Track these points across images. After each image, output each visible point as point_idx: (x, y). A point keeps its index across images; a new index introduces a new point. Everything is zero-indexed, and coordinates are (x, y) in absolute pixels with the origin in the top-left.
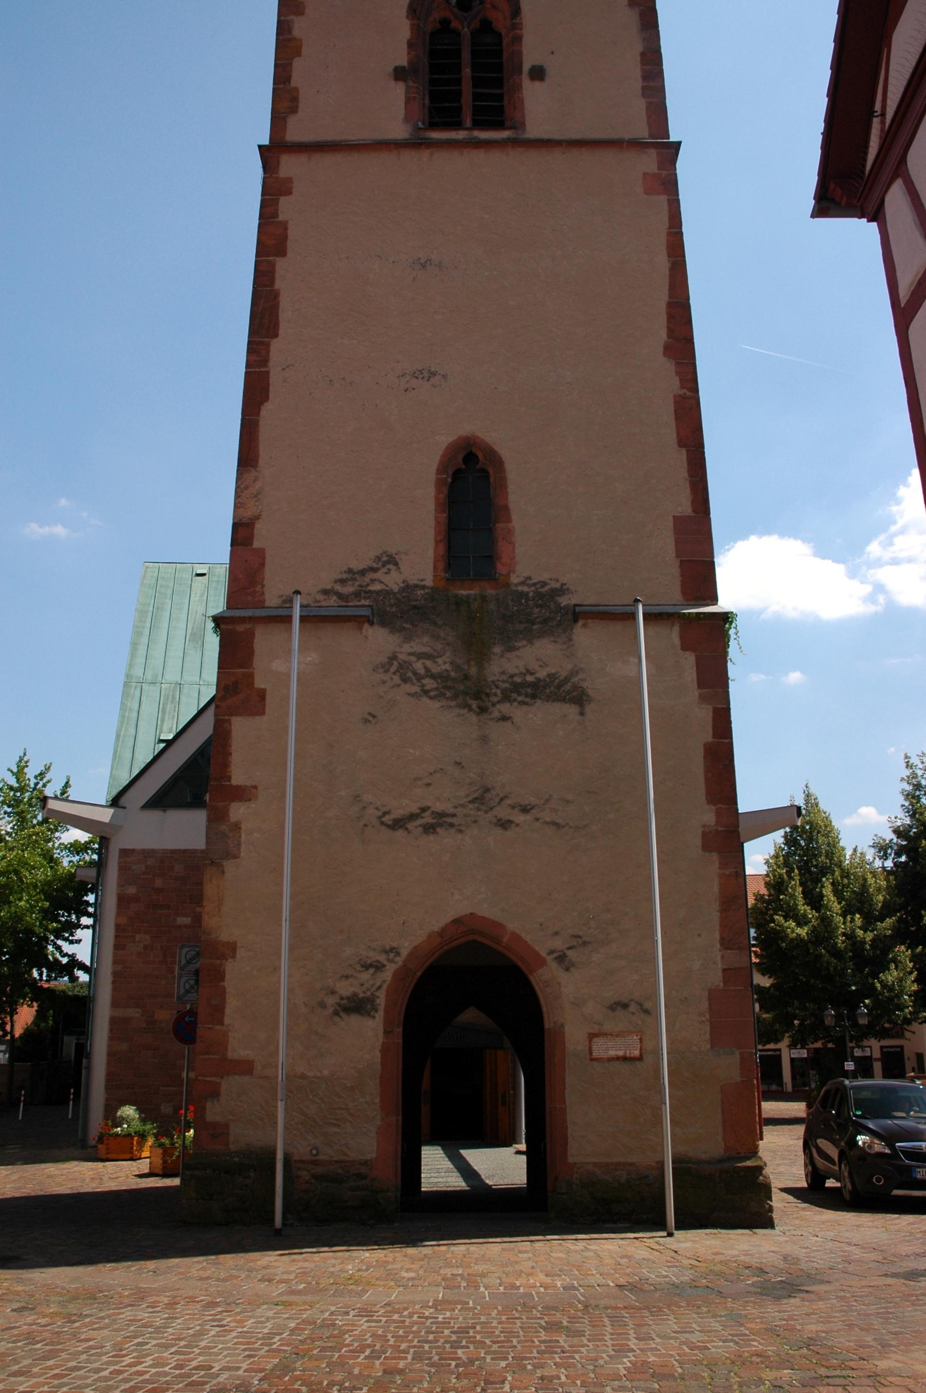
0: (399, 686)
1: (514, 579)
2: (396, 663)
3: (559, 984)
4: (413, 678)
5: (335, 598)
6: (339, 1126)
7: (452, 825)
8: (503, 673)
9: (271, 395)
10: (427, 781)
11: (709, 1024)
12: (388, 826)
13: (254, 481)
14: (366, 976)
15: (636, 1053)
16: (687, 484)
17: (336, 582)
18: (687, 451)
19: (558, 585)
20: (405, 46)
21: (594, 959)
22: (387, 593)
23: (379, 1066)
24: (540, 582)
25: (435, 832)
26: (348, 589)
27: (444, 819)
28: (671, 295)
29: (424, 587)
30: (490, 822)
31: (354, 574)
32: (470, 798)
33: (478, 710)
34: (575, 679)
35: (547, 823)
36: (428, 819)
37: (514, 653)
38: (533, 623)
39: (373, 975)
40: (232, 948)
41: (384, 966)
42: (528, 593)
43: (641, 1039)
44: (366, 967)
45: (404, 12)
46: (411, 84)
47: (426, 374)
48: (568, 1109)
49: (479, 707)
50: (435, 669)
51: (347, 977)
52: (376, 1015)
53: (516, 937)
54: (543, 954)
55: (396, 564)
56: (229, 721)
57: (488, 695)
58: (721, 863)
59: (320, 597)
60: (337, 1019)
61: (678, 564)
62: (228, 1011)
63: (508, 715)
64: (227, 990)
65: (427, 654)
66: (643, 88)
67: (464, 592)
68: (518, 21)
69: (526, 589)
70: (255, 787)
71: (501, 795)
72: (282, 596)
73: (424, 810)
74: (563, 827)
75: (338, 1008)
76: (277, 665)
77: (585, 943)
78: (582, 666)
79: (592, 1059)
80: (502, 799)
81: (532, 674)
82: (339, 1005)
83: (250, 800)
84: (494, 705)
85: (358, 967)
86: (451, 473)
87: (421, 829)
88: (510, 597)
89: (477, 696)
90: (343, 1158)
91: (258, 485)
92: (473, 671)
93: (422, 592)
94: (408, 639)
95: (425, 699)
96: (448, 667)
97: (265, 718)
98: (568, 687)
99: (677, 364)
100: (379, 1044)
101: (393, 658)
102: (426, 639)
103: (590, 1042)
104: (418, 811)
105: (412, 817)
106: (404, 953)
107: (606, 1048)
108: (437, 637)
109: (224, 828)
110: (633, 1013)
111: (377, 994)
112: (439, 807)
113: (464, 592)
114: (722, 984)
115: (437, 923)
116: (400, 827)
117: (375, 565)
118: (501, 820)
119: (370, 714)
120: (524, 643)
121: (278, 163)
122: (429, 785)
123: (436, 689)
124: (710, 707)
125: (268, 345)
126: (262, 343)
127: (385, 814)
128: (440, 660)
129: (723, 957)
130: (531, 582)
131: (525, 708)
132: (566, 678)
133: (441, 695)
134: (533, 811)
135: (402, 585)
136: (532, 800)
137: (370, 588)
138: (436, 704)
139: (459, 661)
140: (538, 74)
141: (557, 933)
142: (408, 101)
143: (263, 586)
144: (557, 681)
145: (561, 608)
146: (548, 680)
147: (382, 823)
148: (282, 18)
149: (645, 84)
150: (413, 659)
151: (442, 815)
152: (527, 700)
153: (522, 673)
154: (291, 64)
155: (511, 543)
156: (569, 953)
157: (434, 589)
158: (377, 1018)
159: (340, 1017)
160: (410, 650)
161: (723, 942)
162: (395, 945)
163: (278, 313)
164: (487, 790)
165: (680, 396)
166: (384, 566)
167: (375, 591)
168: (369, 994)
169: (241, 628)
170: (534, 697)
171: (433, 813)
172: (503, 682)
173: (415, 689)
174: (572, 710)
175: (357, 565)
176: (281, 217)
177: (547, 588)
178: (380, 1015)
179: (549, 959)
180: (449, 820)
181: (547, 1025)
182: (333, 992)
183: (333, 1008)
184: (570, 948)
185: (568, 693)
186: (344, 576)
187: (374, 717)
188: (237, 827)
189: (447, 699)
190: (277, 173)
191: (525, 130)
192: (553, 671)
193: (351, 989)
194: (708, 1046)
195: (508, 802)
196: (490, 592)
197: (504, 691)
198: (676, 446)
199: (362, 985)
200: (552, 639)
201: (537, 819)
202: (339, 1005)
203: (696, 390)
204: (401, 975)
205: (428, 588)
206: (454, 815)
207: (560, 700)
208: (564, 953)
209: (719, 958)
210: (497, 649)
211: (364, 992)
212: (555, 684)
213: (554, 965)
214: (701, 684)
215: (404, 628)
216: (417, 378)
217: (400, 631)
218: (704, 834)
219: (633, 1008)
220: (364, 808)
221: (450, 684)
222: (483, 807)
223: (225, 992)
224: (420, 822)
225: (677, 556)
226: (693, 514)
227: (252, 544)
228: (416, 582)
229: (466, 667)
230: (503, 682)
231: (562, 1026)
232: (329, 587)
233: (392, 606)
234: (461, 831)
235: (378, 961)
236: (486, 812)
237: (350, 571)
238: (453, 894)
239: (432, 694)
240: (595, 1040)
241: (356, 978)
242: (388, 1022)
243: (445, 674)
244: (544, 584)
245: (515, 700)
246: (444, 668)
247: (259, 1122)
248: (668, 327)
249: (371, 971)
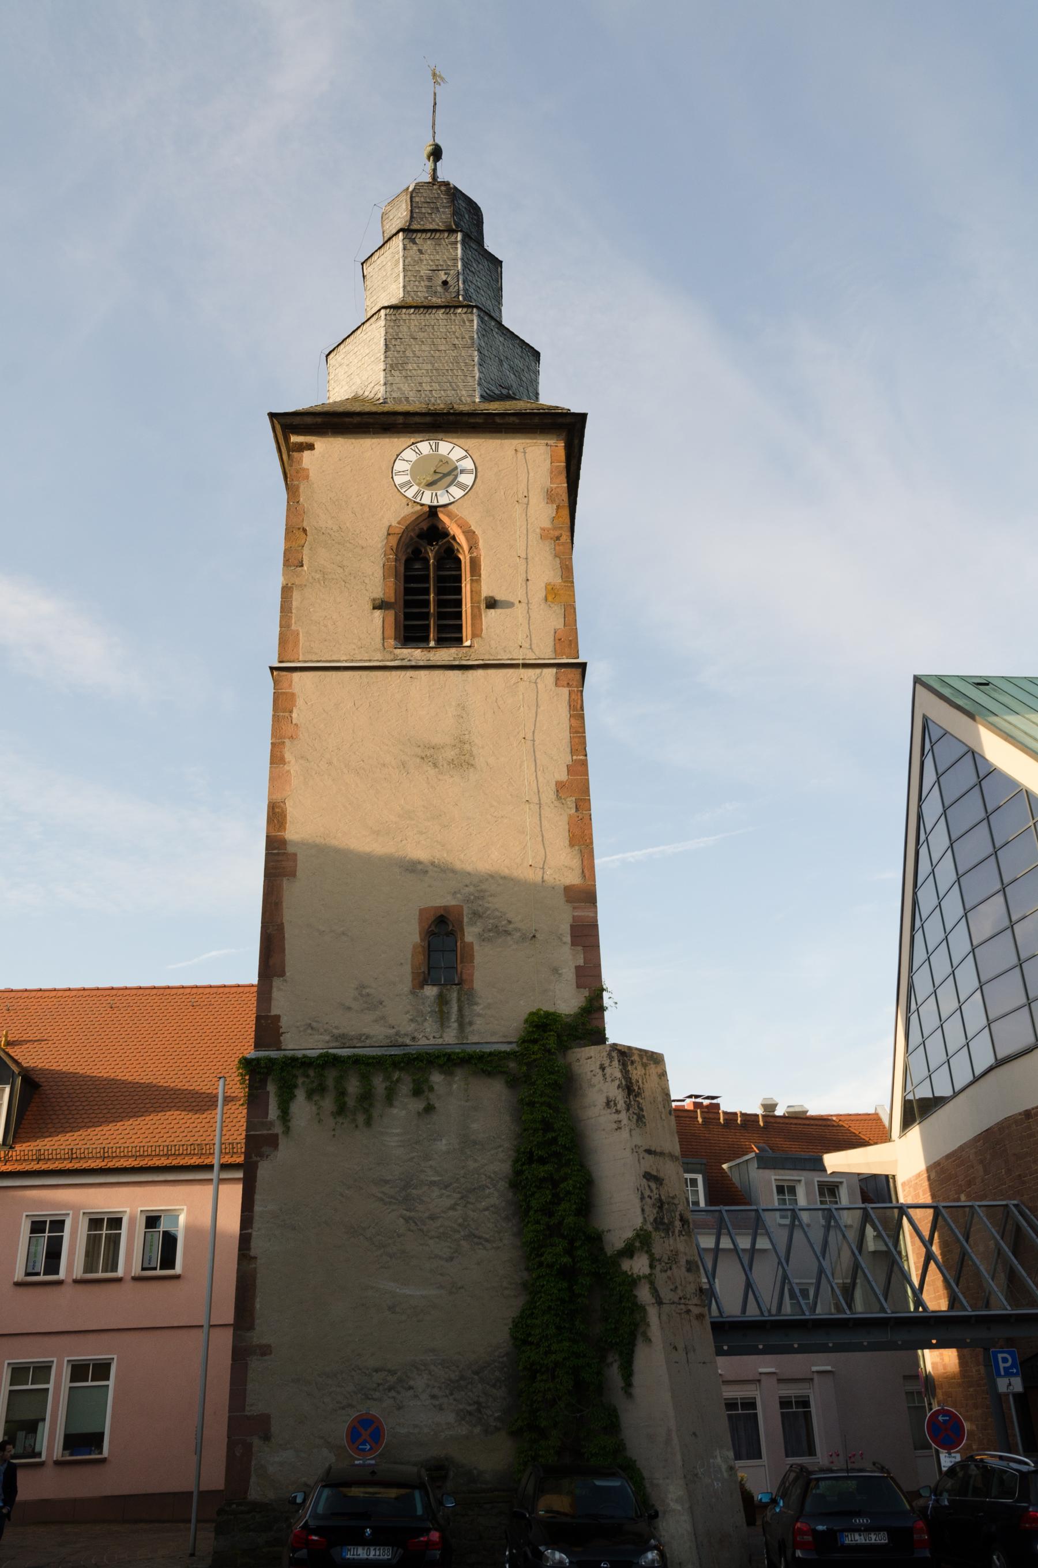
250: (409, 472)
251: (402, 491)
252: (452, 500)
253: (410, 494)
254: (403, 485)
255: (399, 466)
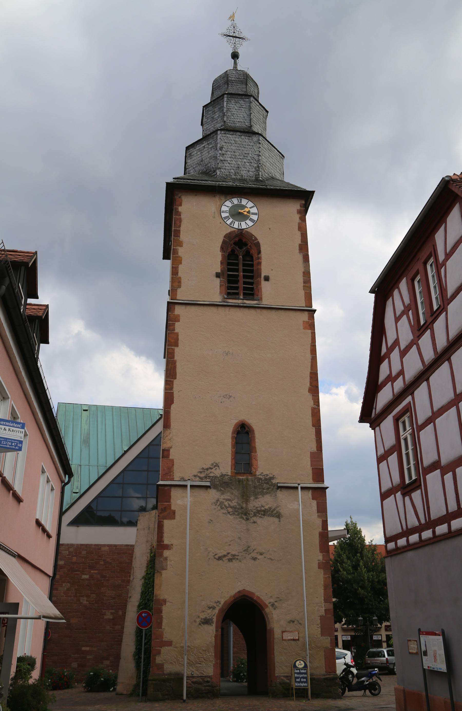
0: (220, 510)
1: (258, 473)
2: (219, 502)
3: (272, 614)
4: (225, 507)
5: (198, 478)
6: (200, 664)
7: (237, 559)
8: (254, 506)
9: (174, 401)
10: (230, 544)
11: (320, 628)
12: (217, 559)
13: (169, 434)
14: (209, 611)
15: (297, 638)
16: (315, 440)
17: (198, 472)
18: (315, 428)
19: (272, 476)
20: (220, 263)
21: (283, 605)
22: (216, 477)
23: (214, 643)
24: (266, 474)
25: (232, 561)
26: (202, 475)
27: (235, 557)
28: (311, 369)
29: (228, 475)
30: (250, 558)
31: (204, 470)
32: (243, 550)
33: (246, 519)
34: (277, 509)
35: (269, 559)
36: (229, 556)
37: (258, 500)
38: (264, 489)
39: (212, 610)
40: (165, 601)
41: (215, 608)
42: (262, 478)
43: (298, 633)
44: (210, 608)
45: (219, 249)
46: (222, 279)
47: (228, 396)
48: (275, 657)
49: (246, 518)
50: (232, 505)
51: (203, 612)
52: (213, 625)
53: (258, 597)
54: (267, 603)
55: (218, 467)
56: (163, 521)
57: (249, 514)
58: (324, 573)
59: (193, 478)
60: (200, 626)
61: (311, 469)
62: (163, 624)
63: (256, 521)
64: (163, 617)
65: (229, 499)
66: (304, 286)
67: (241, 478)
68: (260, 256)
69: (261, 477)
70: (172, 545)
71: (254, 549)
72: (180, 477)
73: (228, 553)
74: (273, 560)
75: (200, 622)
76: (179, 502)
77: (280, 600)
78: (280, 504)
79: (283, 640)
80: (254, 550)
81: (264, 507)
82: (201, 621)
83: (170, 549)
84: (251, 518)
85: (207, 608)
86: (236, 433)
87: (227, 560)
88: (256, 480)
89: (245, 514)
90: (202, 675)
91: (171, 435)
92: (244, 505)
93: (227, 477)
94: (223, 494)
95: (229, 515)
96: (236, 504)
97: (175, 521)
98: (275, 512)
99: (313, 396)
100: (214, 635)
101: (218, 500)
102: (229, 494)
103: (282, 634)
104: (227, 554)
105: (225, 556)
106: (222, 603)
107: (287, 636)
108: (232, 494)
109: (162, 559)
110: (296, 624)
111: (213, 617)
112: (233, 553)
113: (241, 478)
114: (324, 615)
115: (233, 592)
116: (221, 559)
117: (211, 467)
118: (253, 558)
119: (210, 520)
120: (261, 496)
121: (174, 309)
122: (230, 545)
123: (232, 511)
124: (321, 519)
125: (173, 382)
126: (171, 381)
127: (216, 555)
128: (233, 502)
129: (324, 605)
130: (263, 474)
131: (261, 519)
132: (274, 509)
133: (234, 514)
134: (263, 554)
135: (220, 474)
136: (263, 551)
137: (210, 475)
138: (231, 517)
139: (239, 502)
140: (267, 279)
141: (271, 597)
142: (221, 286)
143: (173, 473)
144: (272, 510)
145: (273, 484)
146: (269, 509)
147: (215, 558)
148: (175, 248)
149: (304, 285)
150: (224, 501)
151: (234, 555)
152: (262, 516)
153: (260, 507)
154: (178, 267)
155: (257, 460)
156: (275, 603)
157: (231, 476)
158: (213, 626)
159: (201, 625)
160: (224, 498)
161: (324, 599)
162: (219, 600)
163: (176, 369)
164: (249, 547)
165: (313, 408)
166: (214, 467)
167: (211, 476)
168: (210, 617)
169: (166, 488)
170: (264, 515)
171: (231, 554)
172: (254, 509)
173: (225, 511)
174: (276, 520)
175: (205, 467)
176: (176, 331)
177: (268, 477)
178: (214, 625)
179: (269, 605)
180: (237, 557)
181: (268, 628)
182: (199, 617)
183: (199, 623)
184: (276, 602)
185: (275, 514)
186: (201, 470)
187: (212, 521)
188: (166, 559)
189: (236, 515)
190: (174, 312)
191: (262, 301)
192: (270, 506)
193: (205, 616)
194: (320, 636)
195: (255, 551)
196: (250, 477)
197: (254, 513)
198: (312, 426)
199: (208, 614)
200: (270, 495)
201: (265, 557)
202: (201, 621)
203: (318, 405)
204: (220, 611)
205: (229, 476)
206: (238, 556)
207: (273, 516)
208: (274, 604)
209: (323, 606)
210: (252, 498)
211: (209, 617)
212: (271, 511)
213: (271, 607)
214: (318, 511)
215: (221, 490)
216: (225, 398)
217: (220, 491)
218: (319, 563)
219: (296, 622)
220: (209, 553)
221: (237, 510)
222: (247, 553)
223: (162, 617)
224: (227, 558)
225: (311, 466)
226: (317, 451)
227: (169, 458)
228: (225, 473)
229: (242, 504)
230: (254, 509)
231: (273, 628)
232: (196, 474)
233: (217, 482)
234: (240, 561)
235: (214, 606)
236: (249, 555)
237: (203, 468)
238: (238, 583)
239: (231, 513)
240: (284, 633)
241: (206, 612)
242: (217, 627)
243: (235, 506)
244: (267, 475)
245: (258, 516)
246: (235, 504)
247: (174, 663)
248: (310, 382)
249: (211, 609)
250: (228, 212)
251: (225, 221)
252: (248, 227)
253: (229, 222)
254: (226, 218)
255: (224, 208)
